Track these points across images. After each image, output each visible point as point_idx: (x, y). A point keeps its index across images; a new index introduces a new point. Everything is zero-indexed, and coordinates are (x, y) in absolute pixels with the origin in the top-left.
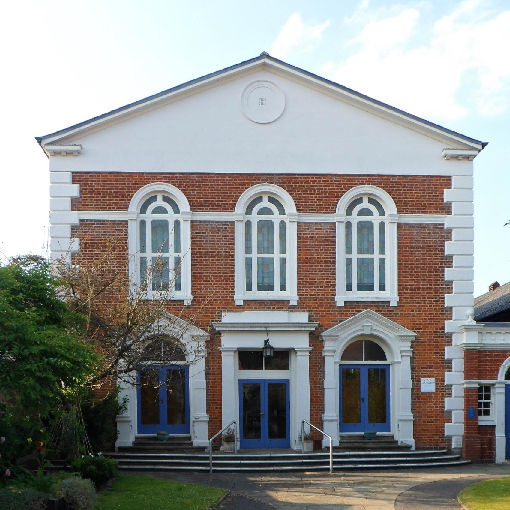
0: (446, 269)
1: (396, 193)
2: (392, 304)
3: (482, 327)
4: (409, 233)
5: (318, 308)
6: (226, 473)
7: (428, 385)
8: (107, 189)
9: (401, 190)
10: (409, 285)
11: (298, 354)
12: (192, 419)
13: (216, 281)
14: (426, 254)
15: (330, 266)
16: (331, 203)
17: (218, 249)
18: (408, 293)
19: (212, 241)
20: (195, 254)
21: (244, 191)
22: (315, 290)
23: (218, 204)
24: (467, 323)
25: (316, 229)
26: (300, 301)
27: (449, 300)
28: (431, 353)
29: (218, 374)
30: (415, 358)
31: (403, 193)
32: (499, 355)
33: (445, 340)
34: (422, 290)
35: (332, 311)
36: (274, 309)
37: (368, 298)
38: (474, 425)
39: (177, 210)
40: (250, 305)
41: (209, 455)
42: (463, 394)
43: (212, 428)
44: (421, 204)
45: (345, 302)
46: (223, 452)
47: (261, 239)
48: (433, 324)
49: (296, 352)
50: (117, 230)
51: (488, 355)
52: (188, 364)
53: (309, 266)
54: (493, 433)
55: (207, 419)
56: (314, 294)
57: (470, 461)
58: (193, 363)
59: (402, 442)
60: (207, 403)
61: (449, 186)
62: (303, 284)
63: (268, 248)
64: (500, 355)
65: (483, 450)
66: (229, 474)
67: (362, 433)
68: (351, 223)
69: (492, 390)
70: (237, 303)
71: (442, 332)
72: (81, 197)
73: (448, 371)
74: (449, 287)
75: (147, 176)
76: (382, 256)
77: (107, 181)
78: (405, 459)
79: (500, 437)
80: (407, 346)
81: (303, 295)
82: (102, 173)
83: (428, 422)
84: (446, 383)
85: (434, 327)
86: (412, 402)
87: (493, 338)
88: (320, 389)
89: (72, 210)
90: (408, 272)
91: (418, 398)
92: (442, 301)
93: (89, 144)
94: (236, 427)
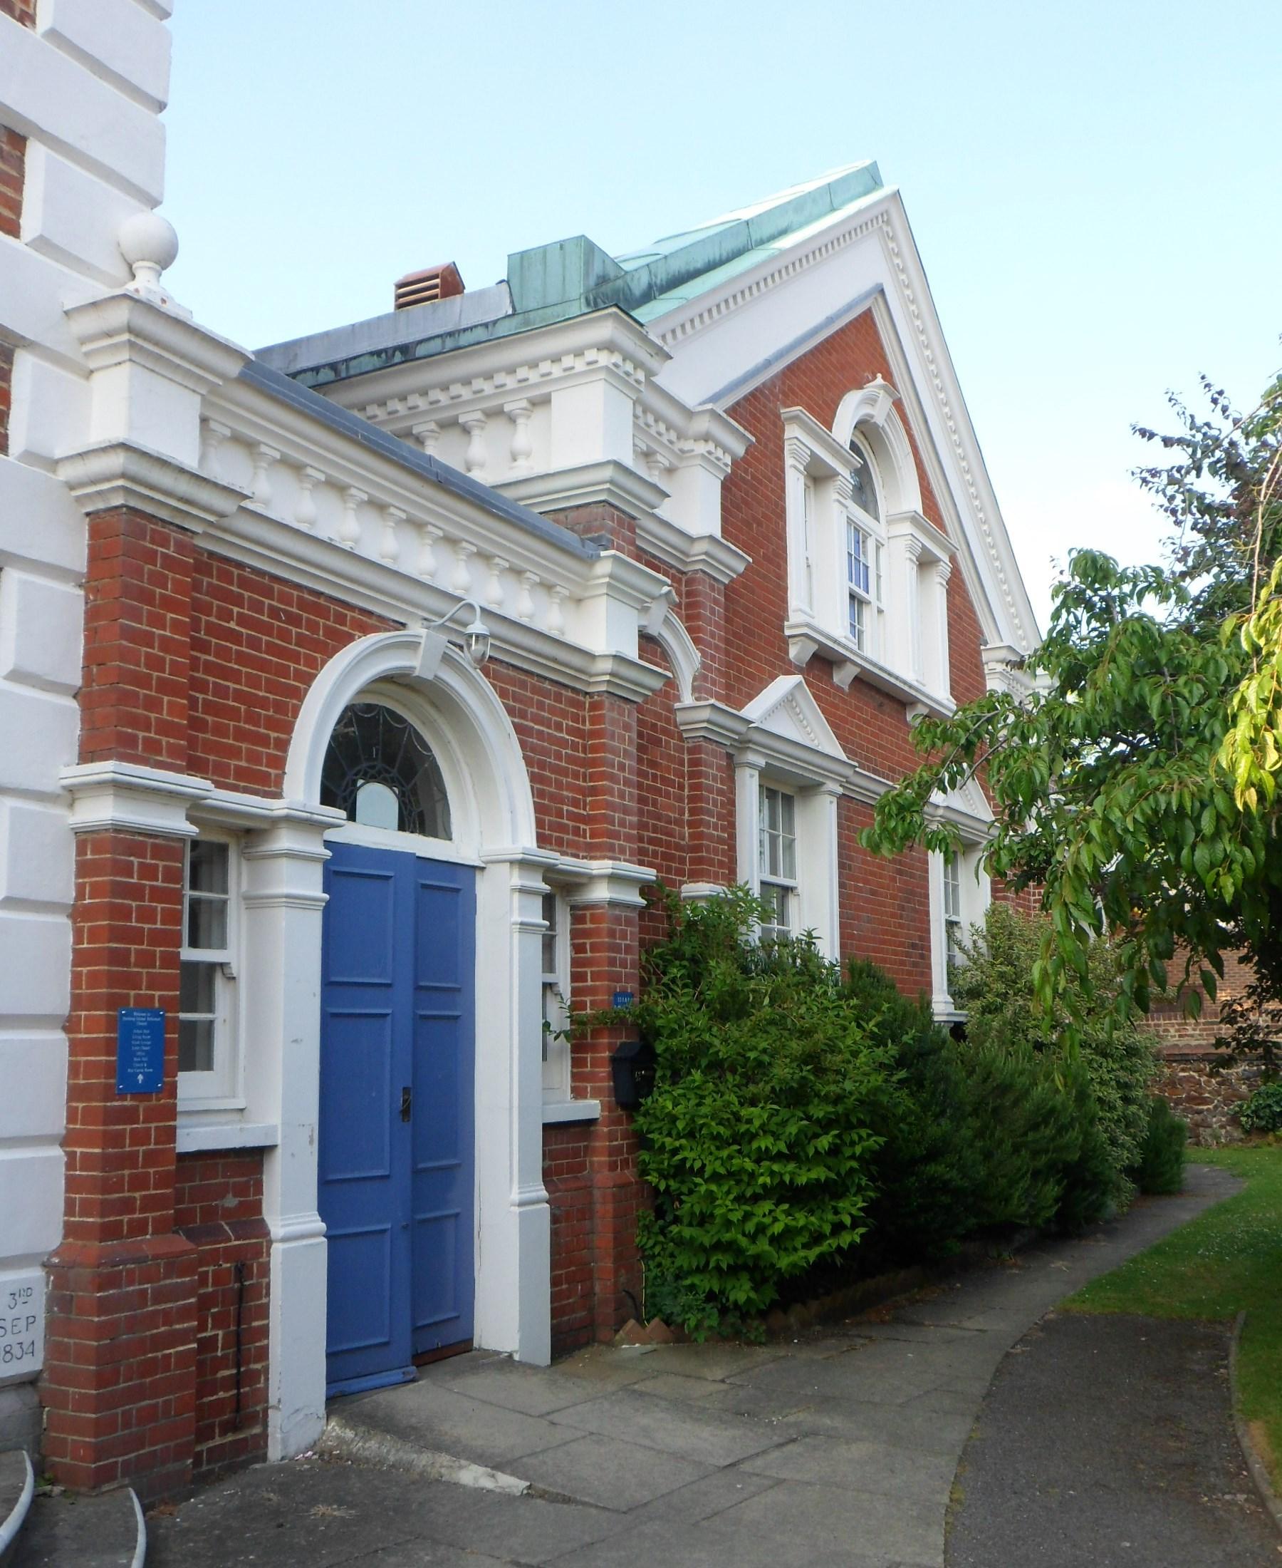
38: (151, 1158)
64: (294, 620)
79: (292, 1220)
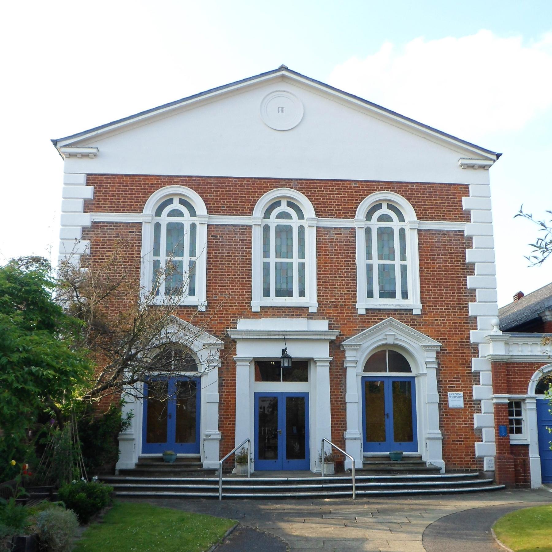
0: (468, 277)
1: (415, 199)
3: (508, 337)
4: (430, 239)
5: (339, 316)
6: (237, 501)
7: (456, 400)
8: (122, 191)
9: (420, 197)
10: (432, 293)
11: (318, 364)
12: (202, 437)
13: (232, 286)
14: (447, 261)
15: (351, 272)
16: (350, 208)
17: (235, 253)
18: (432, 301)
19: (229, 245)
20: (211, 258)
21: (262, 195)
22: (335, 296)
23: (235, 207)
24: (492, 334)
25: (336, 234)
26: (320, 308)
27: (473, 309)
28: (457, 364)
29: (232, 386)
30: (441, 370)
31: (422, 200)
32: (527, 367)
33: (471, 350)
34: (445, 298)
35: (353, 319)
36: (292, 316)
37: (390, 305)
38: (506, 445)
39: (193, 213)
40: (268, 312)
41: (218, 479)
42: (492, 410)
43: (224, 448)
44: (440, 211)
45: (367, 310)
46: (235, 476)
47: (279, 244)
48: (458, 334)
49: (315, 362)
50: (130, 232)
51: (517, 367)
52: (199, 375)
53: (328, 271)
54: (527, 454)
55: (219, 437)
56: (334, 300)
57: (504, 486)
58: (205, 373)
59: (431, 464)
60: (220, 418)
61: (467, 194)
62: (322, 290)
63: (287, 252)
64: (528, 367)
65: (517, 472)
66: (241, 500)
67: (388, 453)
68: (371, 229)
69: (523, 405)
70: (254, 310)
71: (467, 342)
72: (94, 199)
73: (476, 384)
74: (472, 295)
75: (164, 179)
76: (403, 263)
77: (123, 183)
78: (434, 483)
79: (534, 456)
80: (432, 356)
81: (323, 302)
82: (117, 175)
83: (457, 441)
84: (474, 398)
85: (459, 337)
86: (440, 418)
87: (520, 349)
88: (341, 404)
89: (85, 212)
90: (430, 279)
91: (446, 414)
92: (466, 310)
93: (106, 147)
94: (249, 445)
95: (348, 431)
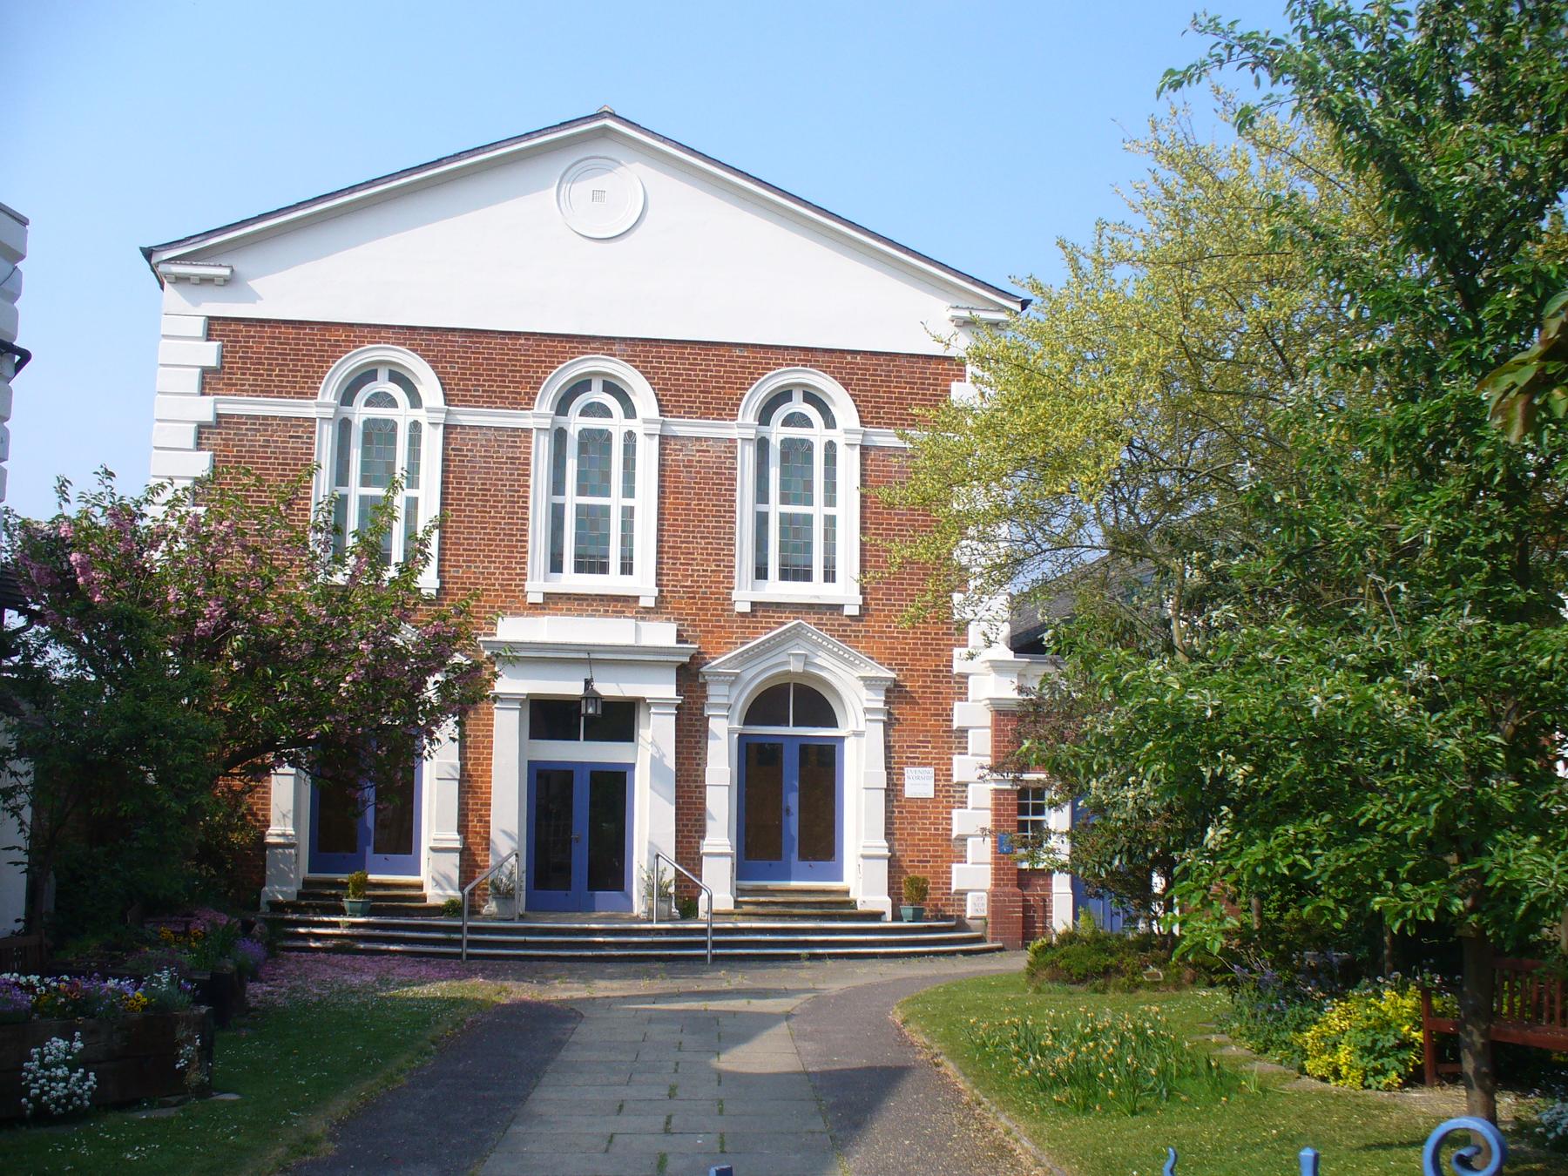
2: (848, 611)
26: (661, 599)
40: (554, 602)
42: (988, 802)
45: (753, 604)
84: (955, 779)
89: (203, 394)
91: (897, 809)
95: (706, 842)
